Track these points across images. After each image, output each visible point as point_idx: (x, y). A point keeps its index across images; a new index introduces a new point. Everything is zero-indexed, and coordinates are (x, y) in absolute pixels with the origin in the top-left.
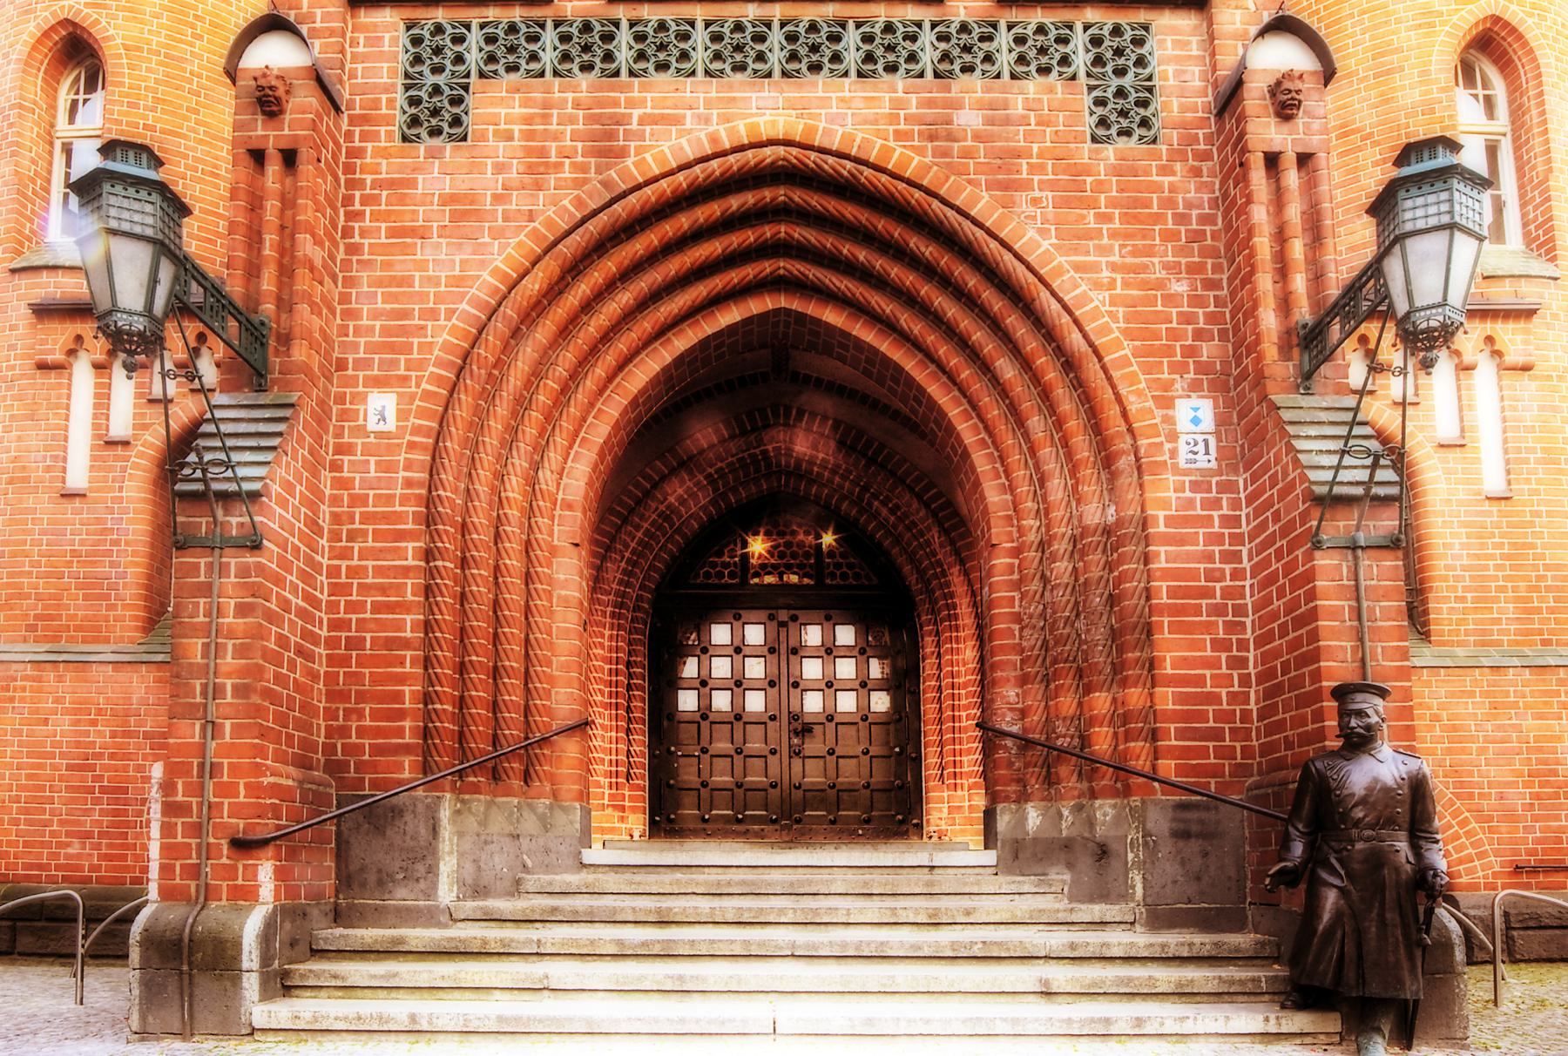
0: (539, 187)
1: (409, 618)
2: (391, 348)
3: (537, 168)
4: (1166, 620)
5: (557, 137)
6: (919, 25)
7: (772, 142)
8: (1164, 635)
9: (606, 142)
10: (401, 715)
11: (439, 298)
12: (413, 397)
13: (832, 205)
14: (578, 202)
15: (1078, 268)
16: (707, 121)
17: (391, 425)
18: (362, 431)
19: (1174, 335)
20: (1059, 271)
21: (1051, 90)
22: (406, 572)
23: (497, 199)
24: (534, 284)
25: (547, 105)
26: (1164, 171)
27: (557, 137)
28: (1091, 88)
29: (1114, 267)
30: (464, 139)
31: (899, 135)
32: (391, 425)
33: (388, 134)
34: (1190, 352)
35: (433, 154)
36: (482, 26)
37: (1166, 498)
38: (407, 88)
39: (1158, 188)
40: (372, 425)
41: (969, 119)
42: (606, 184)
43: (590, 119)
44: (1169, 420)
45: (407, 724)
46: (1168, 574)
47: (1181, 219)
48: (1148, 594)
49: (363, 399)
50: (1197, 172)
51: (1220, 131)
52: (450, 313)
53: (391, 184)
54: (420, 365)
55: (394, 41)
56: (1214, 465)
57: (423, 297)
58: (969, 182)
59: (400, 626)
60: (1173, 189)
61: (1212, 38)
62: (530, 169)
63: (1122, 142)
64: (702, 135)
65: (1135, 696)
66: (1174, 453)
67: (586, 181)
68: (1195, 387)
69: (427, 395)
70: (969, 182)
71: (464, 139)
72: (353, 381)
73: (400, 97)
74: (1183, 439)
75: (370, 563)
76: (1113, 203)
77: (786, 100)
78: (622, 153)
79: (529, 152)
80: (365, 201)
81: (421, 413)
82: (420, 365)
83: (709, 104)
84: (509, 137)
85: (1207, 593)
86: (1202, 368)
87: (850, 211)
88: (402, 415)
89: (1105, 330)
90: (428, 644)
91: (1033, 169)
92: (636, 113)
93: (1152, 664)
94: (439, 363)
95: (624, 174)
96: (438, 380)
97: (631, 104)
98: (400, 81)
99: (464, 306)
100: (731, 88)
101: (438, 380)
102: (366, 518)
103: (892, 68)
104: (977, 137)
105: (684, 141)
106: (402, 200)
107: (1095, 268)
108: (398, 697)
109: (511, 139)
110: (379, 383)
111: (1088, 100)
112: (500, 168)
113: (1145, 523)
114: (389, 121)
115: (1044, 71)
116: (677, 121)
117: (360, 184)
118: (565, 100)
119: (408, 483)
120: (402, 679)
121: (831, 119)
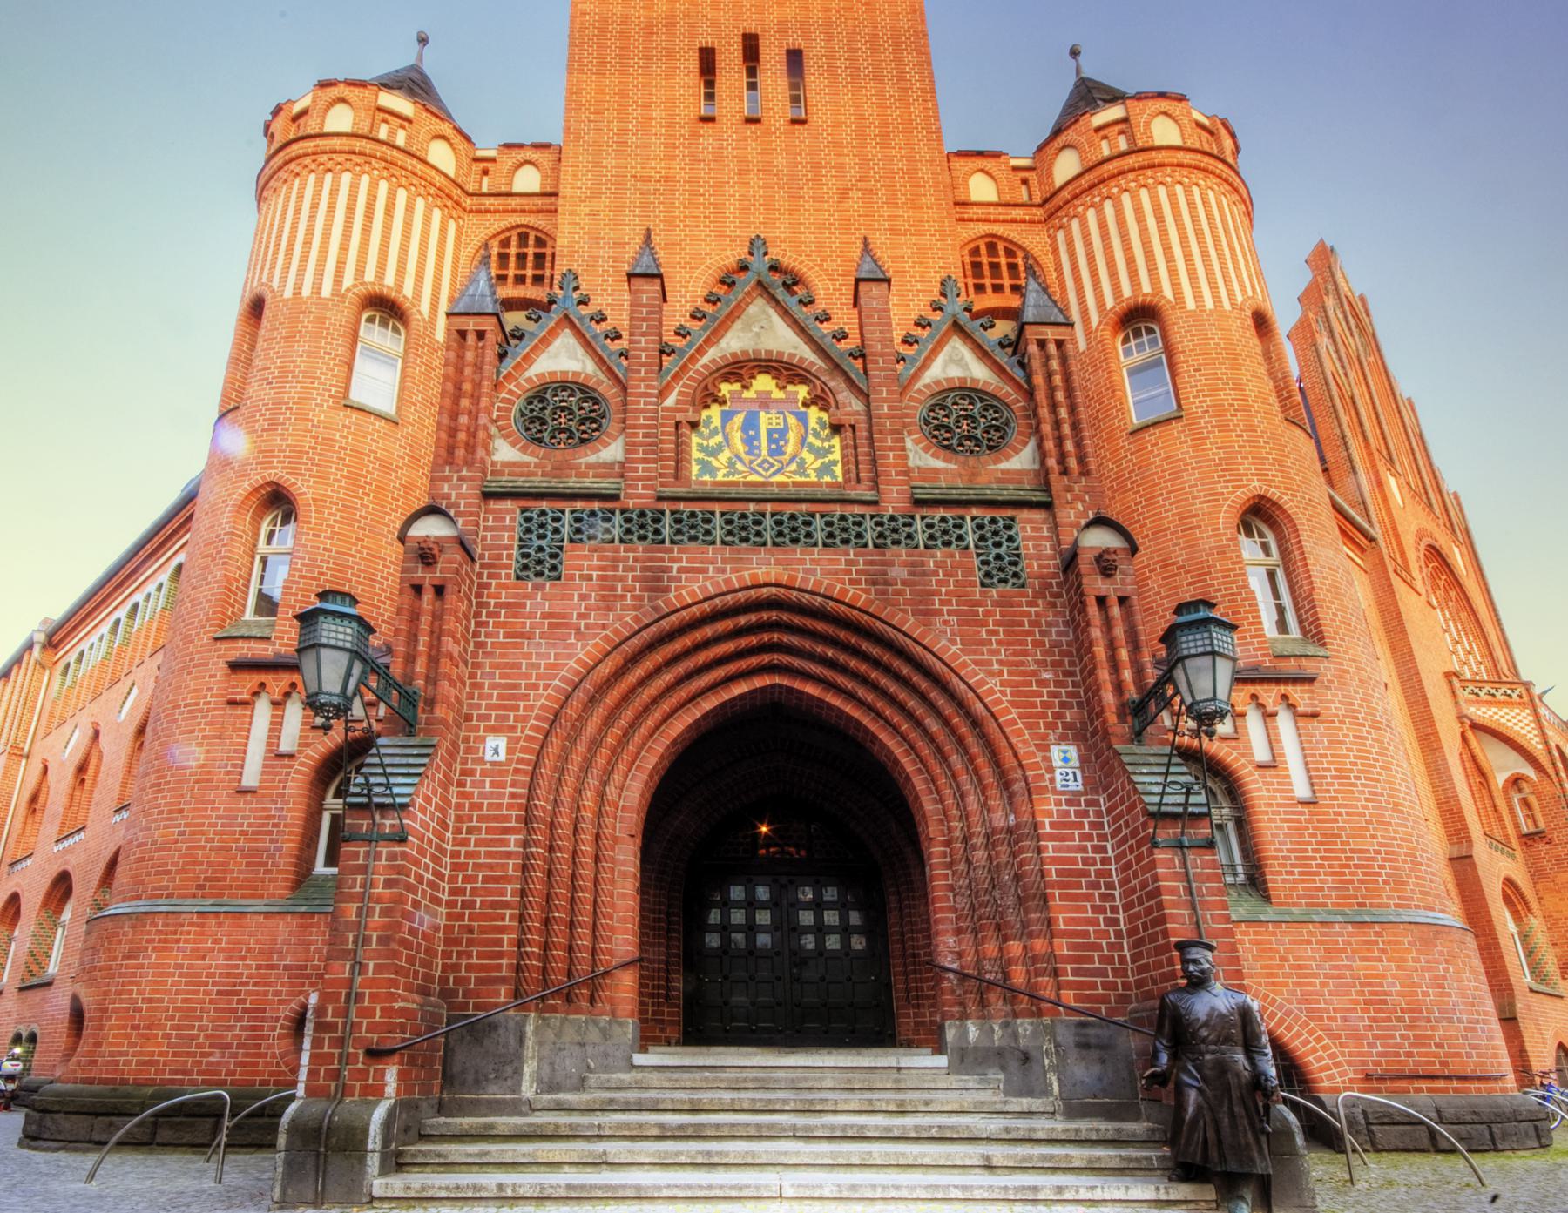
0: (609, 609)
1: (509, 887)
2: (505, 708)
3: (609, 597)
4: (1057, 892)
5: (622, 579)
6: (863, 516)
7: (766, 585)
8: (1057, 902)
9: (655, 582)
10: (500, 955)
11: (539, 677)
12: (518, 739)
14: (636, 619)
15: (976, 663)
16: (723, 571)
17: (502, 757)
18: (481, 761)
19: (1045, 705)
20: (964, 665)
21: (952, 556)
22: (509, 855)
24: (605, 669)
25: (615, 560)
26: (1030, 604)
27: (622, 579)
28: (978, 555)
29: (1000, 662)
30: (559, 578)
31: (852, 582)
32: (502, 757)
33: (507, 575)
34: (1057, 716)
35: (536, 587)
37: (1049, 811)
38: (521, 547)
39: (1028, 614)
40: (489, 756)
41: (898, 572)
42: (656, 609)
43: (643, 569)
44: (1048, 759)
45: (504, 962)
46: (1054, 861)
48: (1042, 874)
49: (483, 740)
50: (1053, 605)
51: (1066, 580)
52: (546, 687)
53: (507, 605)
54: (525, 719)
55: (513, 520)
56: (1081, 788)
57: (527, 676)
59: (502, 892)
60: (1038, 614)
61: (1056, 526)
63: (1001, 587)
65: (1039, 945)
66: (1052, 780)
67: (641, 606)
68: (1062, 739)
69: (528, 738)
71: (559, 578)
72: (477, 729)
73: (515, 552)
74: (1058, 771)
75: (483, 849)
78: (667, 590)
79: (603, 588)
80: (489, 615)
81: (524, 750)
84: (590, 578)
85: (1086, 874)
86: (1066, 726)
87: (820, 626)
88: (510, 751)
89: (998, 702)
90: (523, 905)
91: (942, 602)
92: (675, 566)
93: (1050, 922)
96: (535, 728)
97: (672, 560)
98: (516, 544)
99: (557, 682)
100: (739, 552)
101: (535, 728)
102: (481, 819)
103: (846, 542)
104: (904, 583)
105: (708, 584)
106: (515, 615)
107: (989, 663)
108: (499, 943)
110: (495, 730)
111: (976, 562)
112: (582, 597)
113: (1036, 826)
114: (508, 567)
115: (947, 544)
116: (705, 571)
117: (487, 605)
119: (513, 795)
120: (502, 930)
121: (806, 571)
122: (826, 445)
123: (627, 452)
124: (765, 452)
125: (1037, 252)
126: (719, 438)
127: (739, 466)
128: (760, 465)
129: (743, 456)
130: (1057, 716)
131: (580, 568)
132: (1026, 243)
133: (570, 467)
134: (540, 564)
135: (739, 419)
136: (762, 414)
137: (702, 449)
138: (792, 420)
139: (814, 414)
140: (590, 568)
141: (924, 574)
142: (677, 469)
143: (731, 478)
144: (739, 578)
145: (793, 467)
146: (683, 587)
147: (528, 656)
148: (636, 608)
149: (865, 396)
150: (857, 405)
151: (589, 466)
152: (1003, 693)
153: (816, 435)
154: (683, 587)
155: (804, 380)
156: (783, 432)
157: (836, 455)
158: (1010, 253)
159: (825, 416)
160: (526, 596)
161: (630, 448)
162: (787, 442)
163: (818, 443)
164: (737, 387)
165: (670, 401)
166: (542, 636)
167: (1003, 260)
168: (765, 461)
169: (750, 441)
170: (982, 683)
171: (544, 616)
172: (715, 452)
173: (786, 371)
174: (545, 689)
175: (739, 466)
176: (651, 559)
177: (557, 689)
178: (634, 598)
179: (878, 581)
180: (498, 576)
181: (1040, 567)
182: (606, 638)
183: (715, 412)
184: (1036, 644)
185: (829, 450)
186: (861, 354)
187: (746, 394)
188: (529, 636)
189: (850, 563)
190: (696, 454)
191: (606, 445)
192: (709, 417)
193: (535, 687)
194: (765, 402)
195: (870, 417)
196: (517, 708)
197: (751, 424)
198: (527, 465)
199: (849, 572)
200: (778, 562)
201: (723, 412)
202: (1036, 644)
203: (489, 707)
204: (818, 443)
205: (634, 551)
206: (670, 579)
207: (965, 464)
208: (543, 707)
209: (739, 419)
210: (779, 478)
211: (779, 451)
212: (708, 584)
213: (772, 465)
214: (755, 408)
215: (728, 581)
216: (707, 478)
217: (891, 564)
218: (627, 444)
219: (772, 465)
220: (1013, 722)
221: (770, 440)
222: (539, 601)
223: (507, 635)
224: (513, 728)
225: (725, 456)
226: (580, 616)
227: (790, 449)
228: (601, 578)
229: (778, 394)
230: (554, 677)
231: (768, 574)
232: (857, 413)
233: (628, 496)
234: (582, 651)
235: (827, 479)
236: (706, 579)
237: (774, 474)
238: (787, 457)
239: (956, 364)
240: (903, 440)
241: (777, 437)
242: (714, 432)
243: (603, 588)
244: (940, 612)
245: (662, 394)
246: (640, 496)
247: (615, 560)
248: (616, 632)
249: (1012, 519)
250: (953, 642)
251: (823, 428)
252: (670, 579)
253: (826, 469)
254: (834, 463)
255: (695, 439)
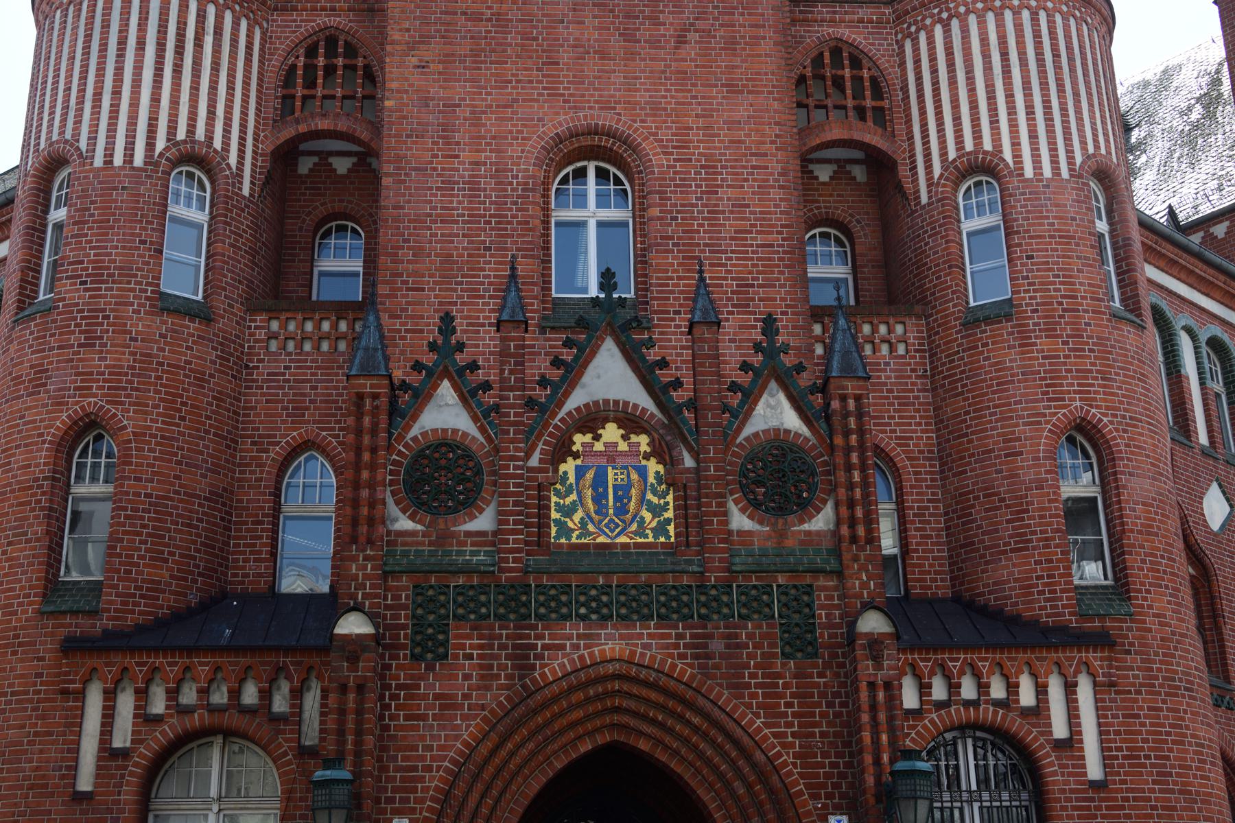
0: (488, 688)
2: (406, 790)
5: (498, 657)
6: (690, 587)
9: (523, 660)
13: (644, 692)
14: (508, 698)
15: (775, 735)
19: (828, 776)
20: (765, 738)
23: (466, 697)
24: (484, 750)
26: (820, 675)
27: (498, 657)
29: (794, 735)
34: (835, 786)
35: (431, 668)
36: (455, 587)
39: (817, 685)
41: (717, 645)
42: (524, 686)
43: (515, 647)
47: (829, 705)
52: (439, 768)
54: (422, 801)
55: (407, 597)
57: (423, 758)
58: (718, 684)
62: (482, 677)
64: (575, 656)
70: (718, 684)
72: (384, 812)
76: (793, 695)
77: (620, 635)
78: (533, 667)
79: (481, 667)
80: (392, 697)
82: (422, 801)
83: (579, 637)
87: (653, 695)
89: (790, 774)
92: (539, 643)
94: (433, 799)
95: (534, 681)
97: (538, 637)
99: (447, 764)
101: (430, 809)
104: (721, 656)
106: (413, 697)
107: (784, 735)
109: (472, 659)
112: (467, 677)
114: (404, 647)
116: (563, 647)
117: (389, 687)
118: (501, 635)
121: (645, 646)
122: (662, 501)
123: (500, 522)
124: (611, 511)
125: (883, 62)
126: (574, 497)
127: (591, 528)
128: (607, 526)
129: (593, 515)
130: (835, 786)
131: (463, 647)
132: (873, 50)
133: (454, 535)
134: (431, 647)
135: (590, 475)
136: (610, 469)
137: (559, 508)
138: (634, 476)
139: (654, 467)
140: (472, 647)
141: (738, 646)
142: (539, 535)
143: (583, 541)
144: (591, 655)
145: (634, 527)
146: (547, 665)
147: (423, 738)
148: (508, 687)
149: (696, 456)
150: (689, 462)
151: (468, 534)
152: (795, 765)
153: (655, 493)
154: (547, 665)
155: (644, 431)
156: (629, 485)
157: (670, 514)
158: (856, 63)
159: (661, 468)
160: (421, 678)
161: (502, 516)
162: (629, 501)
163: (655, 500)
164: (588, 438)
165: (534, 461)
166: (435, 717)
167: (847, 73)
168: (611, 521)
169: (599, 499)
170: (779, 755)
171: (437, 697)
172: (568, 511)
173: (631, 422)
174: (438, 771)
175: (591, 528)
176: (521, 637)
177: (447, 770)
178: (507, 677)
179: (701, 653)
180: (397, 657)
181: (830, 636)
182: (484, 719)
183: (569, 467)
184: (822, 715)
185: (664, 508)
186: (693, 404)
187: (599, 446)
188: (424, 718)
189: (680, 636)
190: (554, 515)
191: (481, 511)
192: (565, 473)
193: (428, 769)
194: (611, 454)
195: (699, 479)
196: (415, 790)
197: (600, 481)
198: (413, 533)
199: (677, 646)
200: (622, 637)
201: (577, 467)
202: (822, 715)
203: (395, 790)
204: (655, 500)
205: (507, 628)
206: (537, 657)
207: (773, 525)
208: (437, 789)
209: (590, 475)
210: (623, 539)
211: (621, 510)
212: (565, 660)
213: (617, 525)
214: (603, 462)
215: (581, 658)
216: (563, 540)
217: (711, 636)
218: (499, 513)
219: (617, 525)
220: (801, 793)
221: (617, 498)
222: (432, 686)
223: (406, 718)
224: (413, 810)
225: (577, 517)
226: (465, 697)
227: (632, 506)
228: (480, 657)
229: (623, 446)
230: (444, 758)
231: (613, 649)
232: (688, 470)
233: (502, 570)
234: (467, 731)
235: (662, 539)
236: (564, 656)
237: (618, 535)
238: (629, 516)
239: (776, 413)
240: (724, 505)
241: (622, 493)
242: (569, 492)
243: (481, 667)
244: (748, 686)
245: (528, 456)
246: (511, 570)
247: (492, 637)
248: (492, 711)
249: (811, 586)
250: (757, 715)
251: (660, 484)
252: (537, 657)
253: (661, 529)
254: (668, 521)
255: (554, 499)
